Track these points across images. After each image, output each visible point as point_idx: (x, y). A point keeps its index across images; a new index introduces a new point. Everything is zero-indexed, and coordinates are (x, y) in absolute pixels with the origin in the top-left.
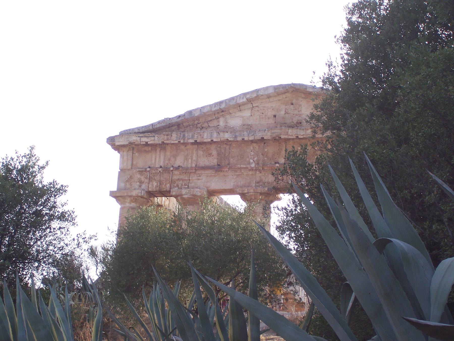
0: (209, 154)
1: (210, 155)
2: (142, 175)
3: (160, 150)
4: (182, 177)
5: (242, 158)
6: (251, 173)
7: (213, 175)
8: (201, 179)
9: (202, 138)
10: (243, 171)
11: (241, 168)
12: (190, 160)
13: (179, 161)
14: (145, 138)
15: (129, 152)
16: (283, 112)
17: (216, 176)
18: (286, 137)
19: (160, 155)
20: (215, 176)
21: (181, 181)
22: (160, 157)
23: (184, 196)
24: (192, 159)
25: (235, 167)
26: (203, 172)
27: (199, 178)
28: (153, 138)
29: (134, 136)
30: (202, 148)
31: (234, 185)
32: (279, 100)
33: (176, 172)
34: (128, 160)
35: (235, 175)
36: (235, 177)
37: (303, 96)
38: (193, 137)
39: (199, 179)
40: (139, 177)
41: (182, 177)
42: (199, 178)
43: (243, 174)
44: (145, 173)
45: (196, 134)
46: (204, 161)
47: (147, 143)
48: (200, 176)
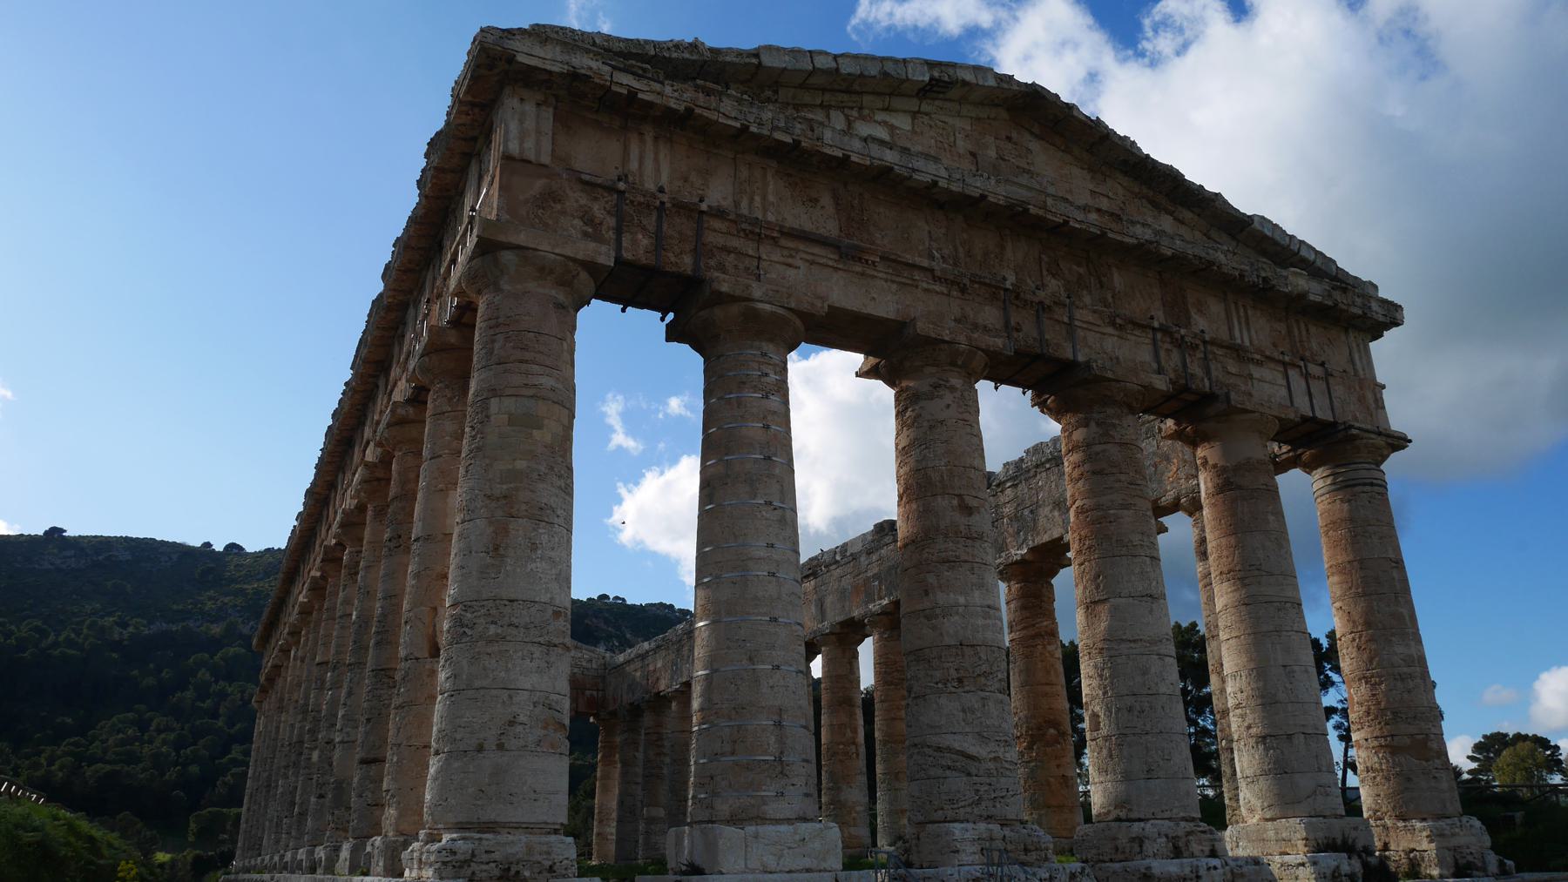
0: (811, 201)
1: (815, 201)
2: (596, 199)
3: (656, 139)
4: (735, 243)
5: (908, 238)
6: (937, 288)
7: (831, 263)
8: (796, 268)
9: (818, 139)
10: (917, 277)
11: (914, 266)
12: (757, 198)
13: (718, 193)
14: (630, 77)
15: (544, 108)
16: (992, 153)
17: (840, 269)
18: (1041, 212)
19: (656, 154)
20: (836, 269)
21: (732, 255)
22: (656, 160)
23: (760, 306)
24: (764, 198)
25: (899, 259)
26: (802, 247)
27: (790, 261)
28: (657, 87)
29: (591, 55)
30: (790, 175)
31: (898, 310)
32: (978, 119)
33: (717, 224)
34: (538, 132)
35: (893, 282)
36: (894, 287)
37: (1036, 130)
38: (786, 131)
39: (790, 265)
40: (583, 202)
41: (735, 243)
42: (790, 261)
43: (917, 287)
44: (606, 194)
45: (800, 123)
46: (797, 216)
47: (633, 94)
48: (791, 256)
